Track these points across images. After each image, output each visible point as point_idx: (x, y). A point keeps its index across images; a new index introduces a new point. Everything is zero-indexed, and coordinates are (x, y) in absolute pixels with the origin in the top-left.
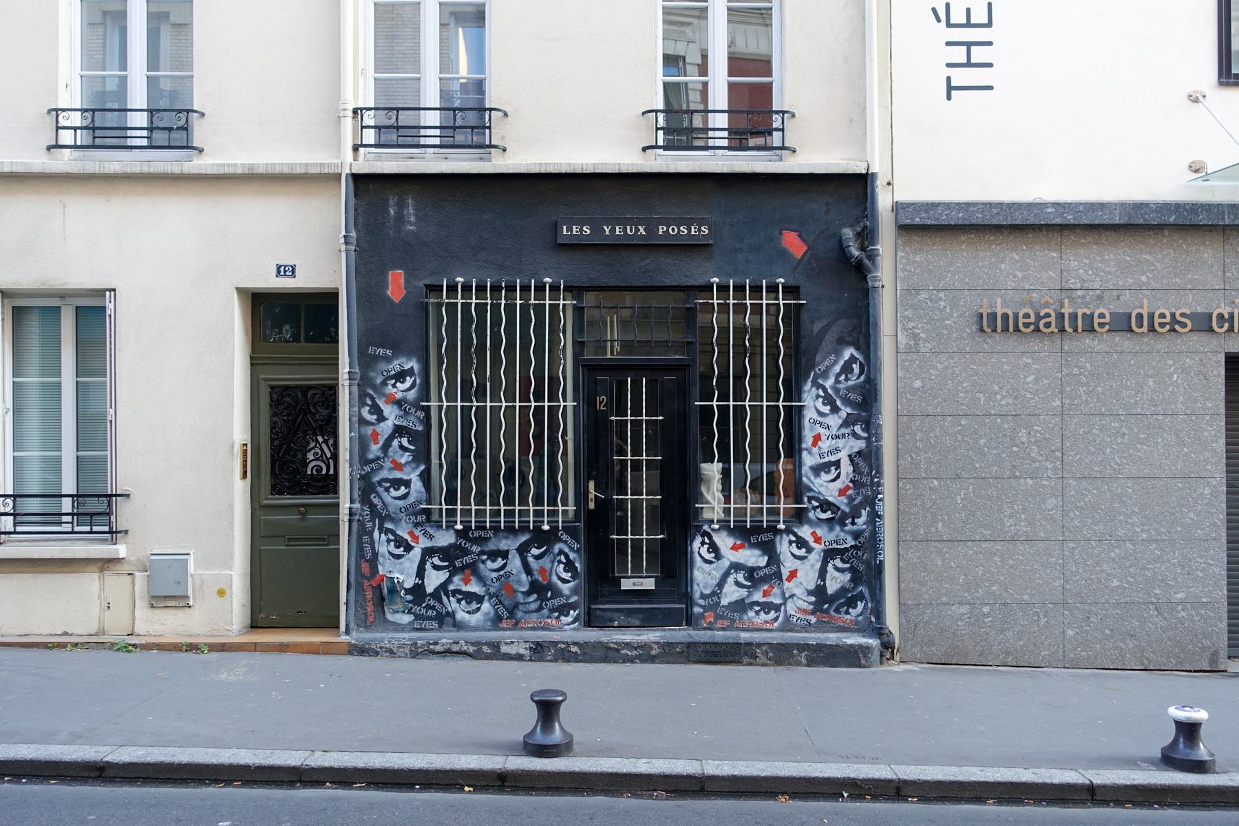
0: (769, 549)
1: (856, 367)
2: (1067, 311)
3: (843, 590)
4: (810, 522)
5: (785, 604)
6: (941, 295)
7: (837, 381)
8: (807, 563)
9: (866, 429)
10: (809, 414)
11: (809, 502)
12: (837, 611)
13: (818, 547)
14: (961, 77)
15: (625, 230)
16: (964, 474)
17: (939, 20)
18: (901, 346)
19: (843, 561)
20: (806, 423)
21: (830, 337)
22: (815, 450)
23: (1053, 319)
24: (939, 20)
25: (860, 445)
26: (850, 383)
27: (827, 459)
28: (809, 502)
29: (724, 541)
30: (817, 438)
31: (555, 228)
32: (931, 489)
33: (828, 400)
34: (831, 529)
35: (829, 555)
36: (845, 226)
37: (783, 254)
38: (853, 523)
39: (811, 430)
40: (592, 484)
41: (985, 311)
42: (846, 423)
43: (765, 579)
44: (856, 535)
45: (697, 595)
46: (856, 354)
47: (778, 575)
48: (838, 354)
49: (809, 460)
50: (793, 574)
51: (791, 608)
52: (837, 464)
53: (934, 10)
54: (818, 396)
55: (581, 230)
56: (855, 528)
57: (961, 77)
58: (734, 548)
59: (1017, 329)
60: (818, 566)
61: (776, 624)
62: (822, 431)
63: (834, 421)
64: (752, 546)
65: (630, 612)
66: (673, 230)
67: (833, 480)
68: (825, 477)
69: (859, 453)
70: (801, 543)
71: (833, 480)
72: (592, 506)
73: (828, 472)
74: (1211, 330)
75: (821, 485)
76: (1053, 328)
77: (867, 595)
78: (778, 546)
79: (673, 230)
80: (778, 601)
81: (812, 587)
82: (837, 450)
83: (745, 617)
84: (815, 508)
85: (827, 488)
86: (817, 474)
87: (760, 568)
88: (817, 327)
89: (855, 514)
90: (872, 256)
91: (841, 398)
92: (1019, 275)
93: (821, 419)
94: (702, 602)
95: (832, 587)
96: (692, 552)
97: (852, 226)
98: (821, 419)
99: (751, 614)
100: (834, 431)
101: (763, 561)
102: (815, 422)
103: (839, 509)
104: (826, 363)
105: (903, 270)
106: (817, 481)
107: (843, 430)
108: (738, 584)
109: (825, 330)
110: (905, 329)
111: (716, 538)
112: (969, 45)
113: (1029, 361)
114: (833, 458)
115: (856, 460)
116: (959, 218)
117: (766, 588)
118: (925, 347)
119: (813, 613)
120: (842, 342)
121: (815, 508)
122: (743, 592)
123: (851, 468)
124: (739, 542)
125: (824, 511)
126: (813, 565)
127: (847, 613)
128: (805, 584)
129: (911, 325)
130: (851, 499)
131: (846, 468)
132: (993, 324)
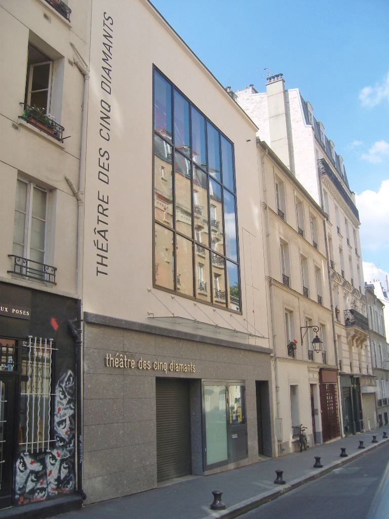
0: (43, 462)
3: (66, 477)
5: (47, 487)
7: (66, 385)
10: (57, 399)
12: (64, 487)
13: (59, 459)
14: (101, 268)
19: (66, 464)
20: (56, 403)
23: (122, 363)
25: (72, 412)
26: (70, 385)
29: (28, 460)
30: (59, 409)
33: (63, 393)
34: (63, 450)
35: (62, 461)
37: (51, 328)
38: (69, 447)
42: (69, 403)
44: (70, 451)
45: (17, 489)
46: (72, 374)
47: (46, 473)
49: (57, 419)
50: (51, 472)
51: (49, 489)
52: (65, 421)
57: (101, 268)
58: (32, 463)
59: (115, 366)
62: (61, 406)
63: (65, 402)
64: (38, 461)
66: (17, 312)
67: (64, 428)
68: (62, 427)
70: (54, 458)
71: (64, 428)
79: (17, 312)
81: (56, 478)
82: (65, 415)
84: (58, 441)
86: (59, 426)
89: (70, 443)
94: (19, 492)
95: (62, 476)
96: (15, 468)
98: (61, 401)
99: (36, 494)
100: (65, 406)
101: (41, 468)
104: (63, 377)
107: (68, 406)
108: (32, 481)
112: (103, 257)
113: (116, 378)
114: (64, 418)
119: (56, 489)
121: (58, 441)
122: (34, 484)
123: (69, 422)
127: (67, 487)
130: (69, 436)
131: (68, 422)
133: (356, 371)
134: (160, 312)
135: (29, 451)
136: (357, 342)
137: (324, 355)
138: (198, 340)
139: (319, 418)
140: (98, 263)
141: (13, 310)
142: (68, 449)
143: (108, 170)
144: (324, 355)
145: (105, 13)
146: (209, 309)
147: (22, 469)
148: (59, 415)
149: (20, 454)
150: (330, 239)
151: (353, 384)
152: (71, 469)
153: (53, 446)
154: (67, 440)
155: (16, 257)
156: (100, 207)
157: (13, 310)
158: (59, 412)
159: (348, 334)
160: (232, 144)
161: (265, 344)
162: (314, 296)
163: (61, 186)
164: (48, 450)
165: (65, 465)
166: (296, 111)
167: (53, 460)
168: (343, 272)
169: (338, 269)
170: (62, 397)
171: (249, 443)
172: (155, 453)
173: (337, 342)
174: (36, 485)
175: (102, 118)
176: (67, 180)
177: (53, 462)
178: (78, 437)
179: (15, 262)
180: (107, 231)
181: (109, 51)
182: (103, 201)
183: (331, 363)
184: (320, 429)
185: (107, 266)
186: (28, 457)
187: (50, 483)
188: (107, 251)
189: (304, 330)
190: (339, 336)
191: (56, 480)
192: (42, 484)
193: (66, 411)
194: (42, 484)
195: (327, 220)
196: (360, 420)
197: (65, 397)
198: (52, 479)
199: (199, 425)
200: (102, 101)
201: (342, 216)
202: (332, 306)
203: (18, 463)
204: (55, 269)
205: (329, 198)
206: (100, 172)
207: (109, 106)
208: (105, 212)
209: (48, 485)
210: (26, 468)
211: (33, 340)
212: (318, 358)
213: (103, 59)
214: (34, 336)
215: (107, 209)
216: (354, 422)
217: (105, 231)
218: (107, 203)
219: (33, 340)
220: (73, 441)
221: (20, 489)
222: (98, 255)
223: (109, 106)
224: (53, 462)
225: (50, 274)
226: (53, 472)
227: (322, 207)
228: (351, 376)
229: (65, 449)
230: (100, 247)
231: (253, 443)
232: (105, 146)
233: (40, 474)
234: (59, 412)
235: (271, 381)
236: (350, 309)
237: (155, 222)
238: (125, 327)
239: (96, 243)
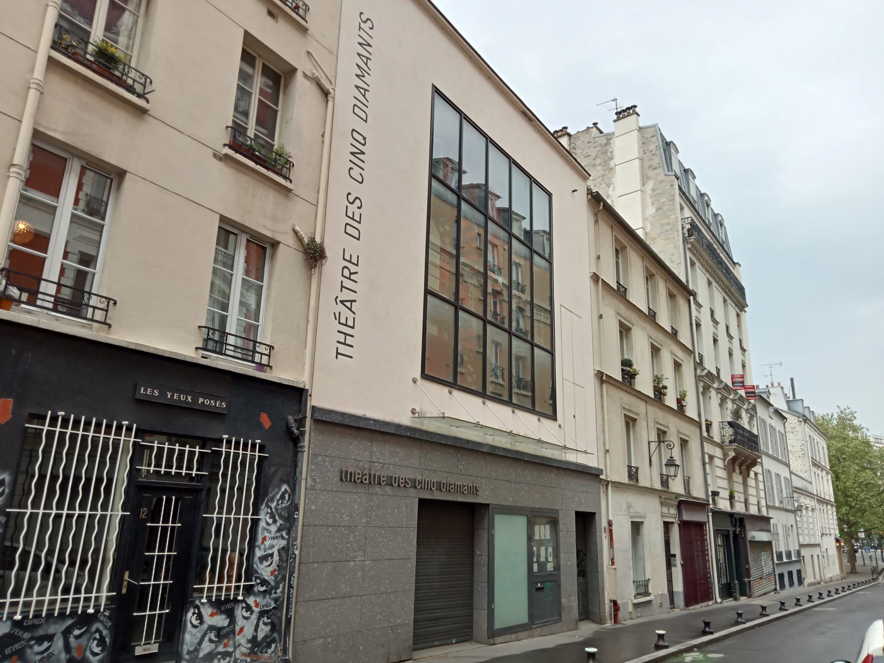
1: (287, 496)
2: (372, 473)
3: (266, 637)
4: (255, 595)
5: (234, 651)
7: (278, 504)
9: (288, 534)
10: (262, 524)
12: (261, 652)
13: (256, 610)
14: (343, 349)
15: (180, 397)
19: (268, 618)
20: (260, 530)
21: (277, 477)
23: (367, 477)
25: (283, 543)
29: (206, 611)
30: (264, 539)
31: (136, 388)
33: (272, 516)
34: (264, 597)
35: (262, 614)
37: (260, 426)
38: (275, 593)
39: (262, 533)
40: (127, 574)
41: (344, 469)
42: (279, 530)
43: (226, 636)
44: (276, 600)
45: (185, 652)
47: (233, 632)
48: (280, 488)
49: (259, 553)
50: (242, 630)
51: (238, 654)
52: (272, 555)
54: (268, 513)
55: (153, 392)
57: (343, 349)
58: (212, 615)
59: (355, 481)
62: (267, 534)
63: (273, 528)
64: (222, 612)
67: (269, 566)
68: (266, 564)
69: (283, 548)
70: (248, 608)
71: (269, 566)
72: (124, 591)
73: (267, 561)
76: (367, 481)
77: (277, 639)
80: (231, 649)
81: (250, 637)
82: (272, 547)
84: (258, 584)
86: (261, 563)
87: (224, 628)
88: (272, 470)
89: (277, 588)
90: (303, 433)
94: (187, 657)
95: (261, 636)
96: (186, 620)
97: (293, 415)
100: (273, 534)
106: (261, 566)
107: (278, 534)
108: (211, 641)
111: (202, 610)
112: (346, 334)
114: (270, 552)
116: (338, 420)
118: (318, 487)
119: (249, 655)
120: (282, 481)
121: (258, 584)
122: (213, 646)
125: (262, 586)
127: (266, 652)
130: (276, 577)
131: (276, 558)
132: (346, 477)
133: (739, 508)
134: (432, 411)
135: (209, 598)
136: (740, 466)
137: (687, 483)
138: (485, 450)
139: (678, 572)
140: (338, 342)
141: (201, 400)
142: (273, 596)
143: (360, 223)
144: (687, 483)
145: (361, 13)
146: (506, 410)
147: (195, 622)
148: (262, 547)
149: (193, 602)
150: (698, 325)
151: (735, 526)
152: (274, 627)
153: (249, 590)
154: (273, 583)
155: (209, 328)
156: (346, 270)
157: (201, 400)
158: (262, 543)
159: (725, 455)
160: (550, 195)
161: (591, 462)
162: (671, 401)
163: (287, 240)
164: (240, 598)
165: (265, 620)
166: (654, 155)
167: (247, 611)
168: (718, 371)
169: (710, 365)
170: (270, 521)
171: (563, 600)
172: (412, 606)
173: (707, 466)
174: (217, 647)
175: (352, 153)
176: (296, 232)
177: (247, 614)
178: (290, 580)
179: (208, 335)
180: (355, 301)
181: (366, 64)
182: (350, 262)
183: (698, 492)
184: (679, 586)
185: (352, 346)
186: (207, 606)
187: (240, 645)
188: (353, 328)
189: (654, 446)
190: (711, 458)
191: (249, 641)
192: (225, 646)
193: (275, 542)
194: (225, 646)
195: (695, 299)
196: (746, 580)
197: (275, 521)
198: (242, 639)
199: (485, 569)
200: (353, 130)
201: (719, 296)
202: (699, 415)
203: (190, 614)
204: (271, 347)
205: (698, 270)
206: (347, 224)
207: (364, 139)
208: (353, 277)
209: (235, 648)
210: (202, 622)
211: (229, 442)
212: (676, 486)
213: (357, 76)
214: (231, 435)
215: (356, 273)
216: (737, 582)
217: (352, 301)
218: (357, 265)
219: (229, 442)
220: (281, 586)
221: (189, 653)
222: (339, 332)
223: (364, 139)
224: (247, 614)
225: (262, 354)
226: (245, 629)
227: (687, 281)
228: (731, 515)
229: (268, 596)
230: (343, 321)
231: (570, 599)
232: (357, 190)
233: (224, 632)
234: (262, 543)
235: (600, 513)
236: (730, 420)
237: (427, 292)
238: (373, 428)
239: (337, 317)
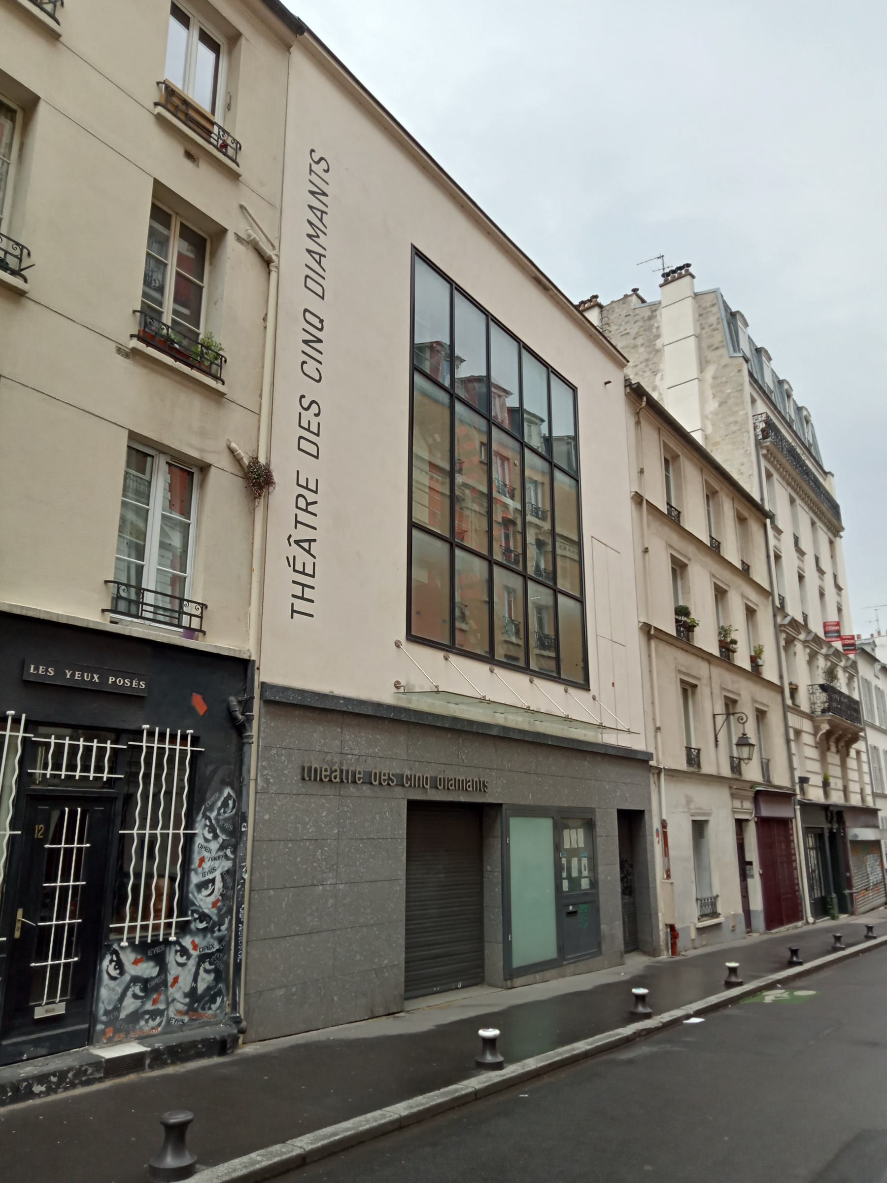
0: (160, 961)
1: (231, 802)
2: (344, 768)
3: (209, 988)
4: (192, 933)
5: (167, 1009)
6: (283, 752)
7: (219, 814)
8: (187, 968)
9: (234, 852)
10: (199, 841)
11: (192, 915)
13: (195, 953)
14: (300, 605)
15: (83, 676)
16: (288, 885)
17: (290, 566)
18: (259, 788)
19: (211, 964)
20: (196, 848)
21: (217, 778)
22: (200, 870)
23: (338, 773)
24: (290, 566)
25: (228, 864)
26: (227, 815)
27: (207, 878)
28: (192, 915)
29: (128, 958)
30: (202, 860)
31: (23, 667)
32: (269, 898)
33: (212, 830)
34: (205, 937)
35: (202, 958)
36: (231, 695)
37: (192, 710)
38: (219, 930)
39: (199, 853)
40: (20, 912)
41: (306, 765)
42: (222, 847)
43: (156, 989)
44: (220, 940)
45: (101, 1012)
46: (232, 793)
47: (165, 983)
48: (221, 793)
49: (195, 879)
50: (176, 980)
51: (171, 1012)
52: (213, 881)
53: (287, 558)
54: (206, 825)
55: (47, 671)
56: (220, 934)
57: (300, 605)
58: (136, 962)
59: (321, 780)
60: (193, 970)
61: (160, 1029)
62: (206, 854)
63: (214, 846)
64: (149, 959)
65: (36, 1043)
66: (120, 682)
67: (210, 895)
68: (205, 892)
69: (228, 871)
71: (210, 895)
72: (17, 935)
73: (207, 888)
74: (371, 783)
75: (201, 900)
76: (338, 780)
77: (224, 991)
78: (167, 956)
79: (120, 682)
80: (162, 1007)
81: (187, 989)
82: (213, 870)
83: (138, 1027)
84: (195, 920)
85: (205, 902)
86: (199, 891)
87: (152, 978)
88: (210, 768)
89: (221, 924)
90: (250, 719)
91: (219, 826)
92: (323, 742)
93: (206, 844)
94: (104, 1018)
95: (201, 987)
96: (101, 971)
97: (235, 695)
98: (206, 844)
99: (142, 1023)
100: (214, 854)
101: (155, 972)
102: (202, 847)
103: (211, 918)
104: (213, 799)
105: (264, 732)
106: (200, 896)
107: (221, 853)
108: (135, 996)
109: (214, 771)
110: (262, 775)
111: (123, 956)
112: (304, 585)
113: (324, 801)
114: (211, 877)
115: (226, 877)
116: (298, 700)
117: (155, 996)
118: (273, 789)
119: (186, 1013)
120: (224, 783)
121: (195, 920)
122: (138, 1003)
123: (221, 885)
124: (139, 957)
125: (201, 922)
126: (190, 970)
127: (210, 1008)
128: (183, 988)
129: (266, 772)
130: (219, 910)
131: (219, 884)
132: (309, 775)
133: (837, 798)
134: (421, 684)
135: (131, 940)
136: (837, 742)
137: (765, 767)
138: (494, 733)
139: (755, 885)
140: (293, 596)
141: (111, 680)
142: (217, 934)
143: (318, 435)
144: (765, 767)
145: (312, 151)
146: (520, 680)
147: (114, 973)
148: (200, 870)
149: (109, 947)
150: (778, 557)
151: (831, 822)
152: (219, 975)
153: (183, 928)
154: (215, 918)
155: (119, 583)
156: (300, 499)
157: (111, 680)
158: (200, 865)
159: (816, 729)
160: (574, 389)
161: (637, 744)
162: (742, 659)
163: (220, 461)
164: (172, 938)
165: (207, 966)
166: (715, 330)
167: (182, 956)
168: (805, 617)
169: (794, 611)
170: (210, 836)
171: (603, 927)
172: (402, 942)
173: (793, 744)
174: (143, 1004)
175: (306, 342)
176: (232, 451)
177: (182, 960)
178: (238, 912)
179: (118, 592)
180: (314, 540)
181: (321, 220)
182: (307, 488)
183: (781, 779)
184: (757, 903)
185: (312, 601)
186: (129, 950)
187: (174, 1000)
188: (313, 576)
189: (720, 720)
190: (798, 733)
191: (186, 995)
192: (155, 1002)
193: (216, 864)
194: (155, 1002)
195: (773, 523)
196: (847, 892)
197: (216, 837)
198: (178, 993)
199: (498, 890)
200: (306, 310)
201: (804, 517)
202: (781, 677)
203: (106, 962)
204: (204, 606)
205: (776, 483)
206: (301, 438)
207: (321, 321)
208: (310, 508)
209: (168, 1004)
210: (122, 972)
211: (151, 734)
212: (752, 773)
213: (309, 236)
214: (153, 724)
215: (316, 503)
216: (834, 895)
217: (310, 541)
218: (316, 492)
219: (151, 734)
220: (227, 921)
221: (107, 1013)
222: (294, 582)
223: (321, 321)
224: (182, 960)
225: (191, 615)
226: (180, 980)
227: (762, 499)
228: (826, 808)
229: (209, 935)
230: (299, 567)
231: (613, 926)
232: (312, 391)
233: (153, 983)
234: (200, 865)
235: (650, 811)
236: (822, 681)
237: (412, 525)
238: (345, 709)
239: (291, 563)
